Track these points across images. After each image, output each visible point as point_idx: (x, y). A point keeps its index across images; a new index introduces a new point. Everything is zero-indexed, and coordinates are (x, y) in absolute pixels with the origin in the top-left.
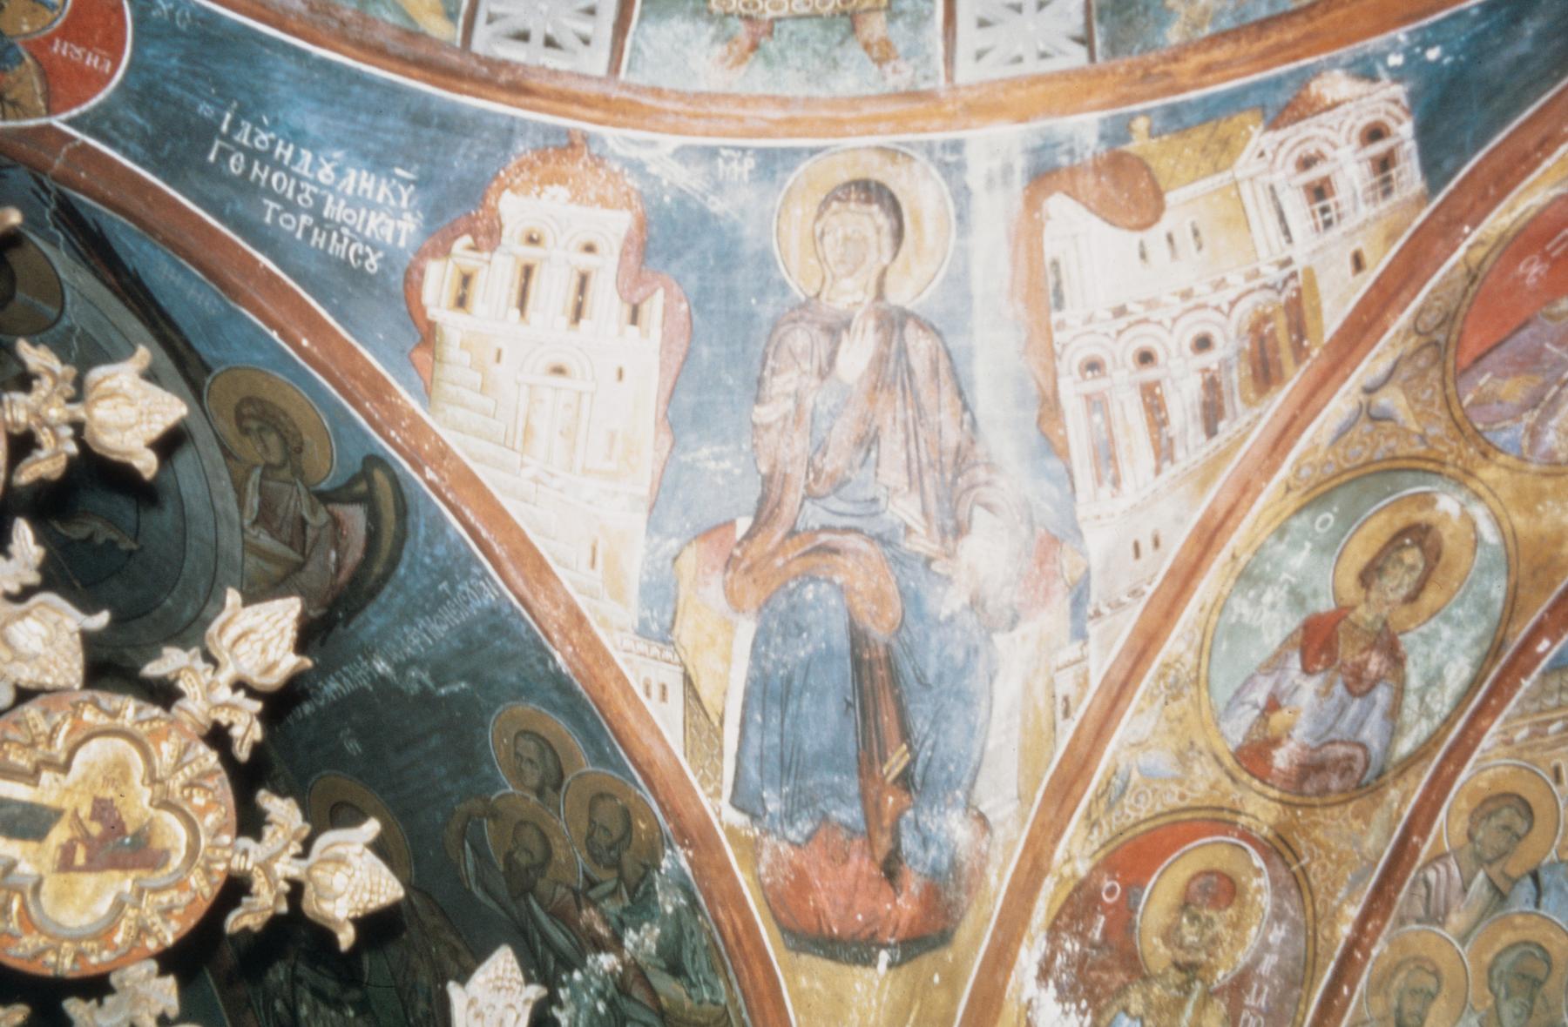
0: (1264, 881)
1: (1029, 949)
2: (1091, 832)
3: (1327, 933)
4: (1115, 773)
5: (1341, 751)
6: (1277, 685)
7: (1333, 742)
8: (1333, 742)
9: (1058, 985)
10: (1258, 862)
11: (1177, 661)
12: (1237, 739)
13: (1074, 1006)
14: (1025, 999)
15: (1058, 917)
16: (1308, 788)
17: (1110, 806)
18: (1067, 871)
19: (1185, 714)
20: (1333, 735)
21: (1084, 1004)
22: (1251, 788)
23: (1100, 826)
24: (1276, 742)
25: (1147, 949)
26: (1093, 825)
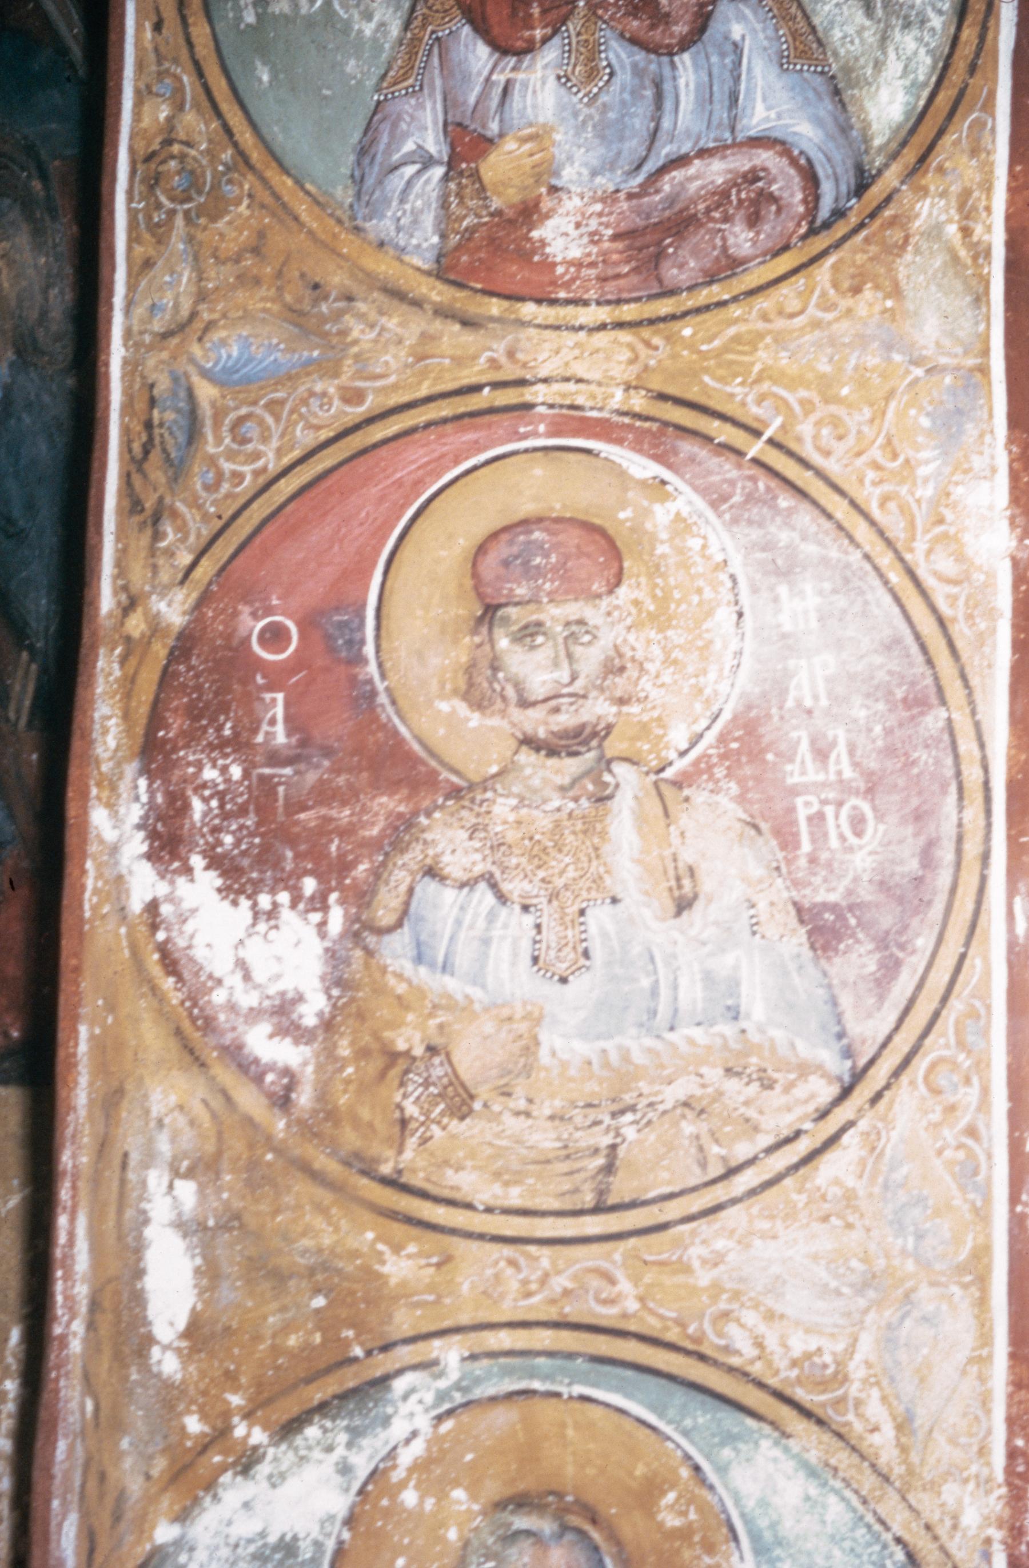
0: (686, 500)
1: (111, 806)
2: (157, 536)
3: (946, 565)
4: (152, 402)
5: (716, 171)
6: (449, 101)
7: (681, 161)
8: (681, 161)
9: (214, 862)
10: (641, 467)
11: (168, 142)
12: (426, 239)
13: (284, 897)
14: (136, 905)
15: (156, 719)
16: (671, 274)
17: (177, 471)
18: (136, 625)
19: (261, 235)
20: (665, 151)
21: (309, 885)
22: (522, 324)
23: (175, 514)
24: (529, 213)
25: (438, 735)
26: (156, 518)
